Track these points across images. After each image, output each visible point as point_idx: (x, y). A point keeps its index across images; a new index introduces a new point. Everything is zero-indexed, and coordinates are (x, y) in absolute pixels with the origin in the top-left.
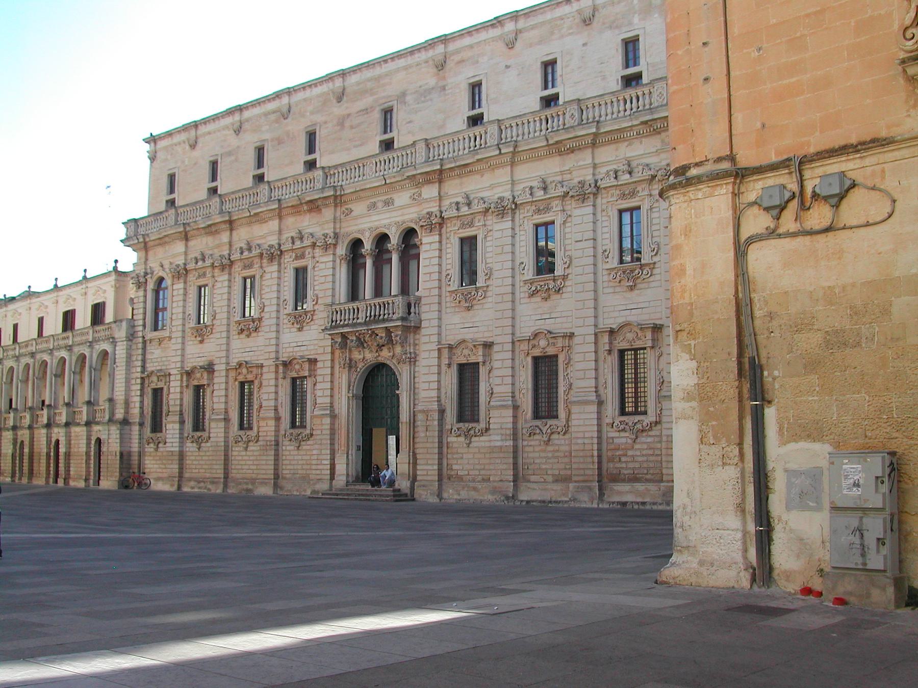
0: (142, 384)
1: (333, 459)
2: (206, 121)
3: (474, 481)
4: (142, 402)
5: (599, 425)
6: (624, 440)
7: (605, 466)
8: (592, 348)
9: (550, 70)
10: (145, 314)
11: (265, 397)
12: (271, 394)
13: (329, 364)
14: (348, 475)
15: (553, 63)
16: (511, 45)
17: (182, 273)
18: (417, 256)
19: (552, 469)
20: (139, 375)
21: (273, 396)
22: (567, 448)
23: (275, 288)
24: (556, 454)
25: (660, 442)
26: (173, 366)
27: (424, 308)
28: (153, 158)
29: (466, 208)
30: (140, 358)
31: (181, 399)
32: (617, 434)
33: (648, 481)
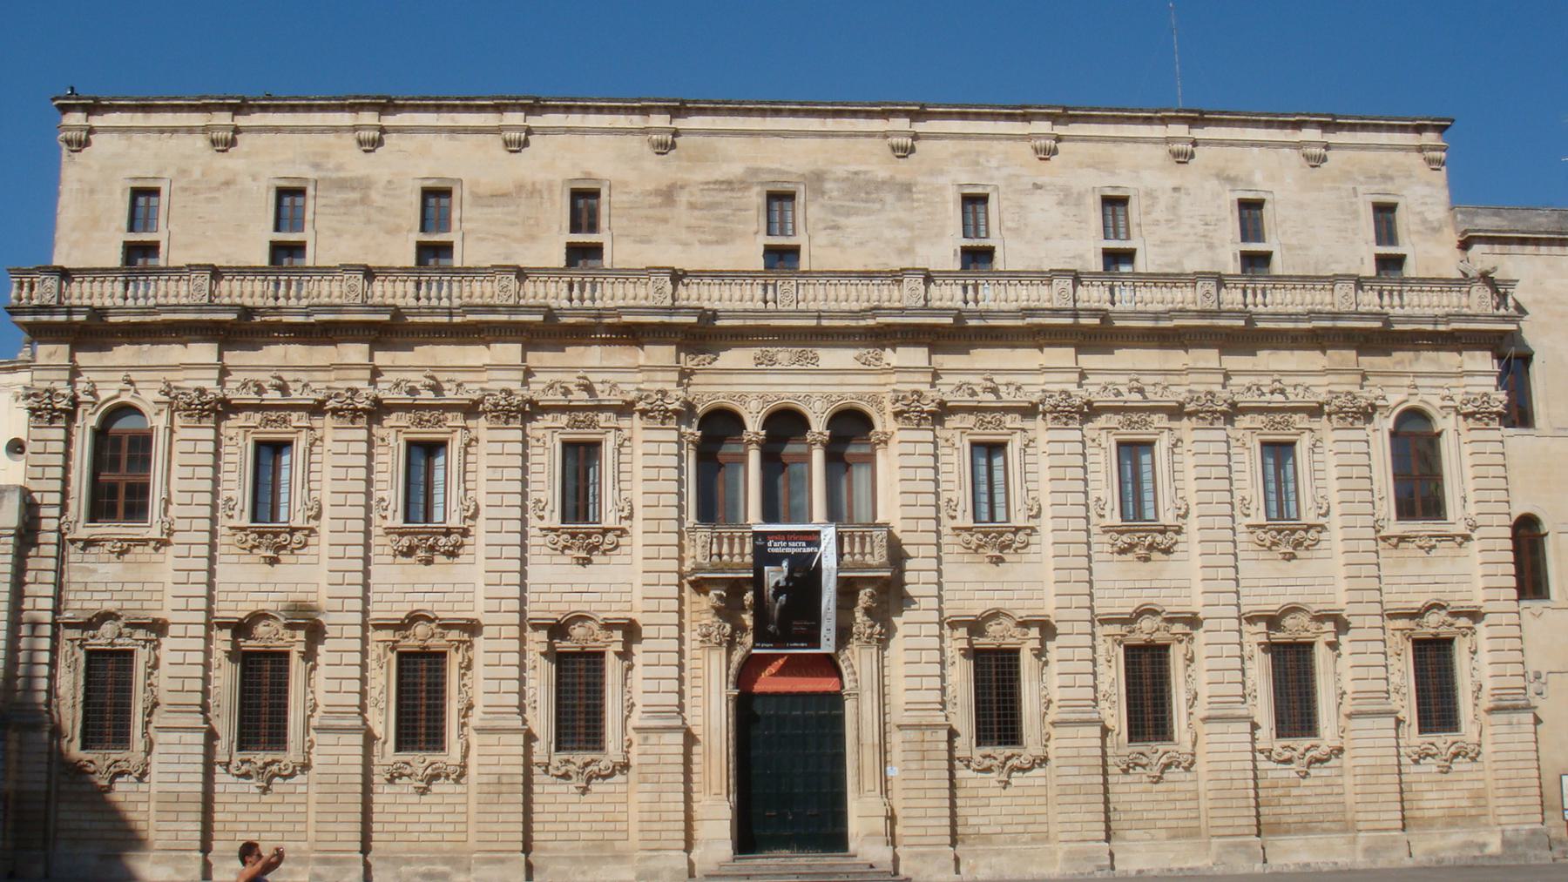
32: (1273, 765)
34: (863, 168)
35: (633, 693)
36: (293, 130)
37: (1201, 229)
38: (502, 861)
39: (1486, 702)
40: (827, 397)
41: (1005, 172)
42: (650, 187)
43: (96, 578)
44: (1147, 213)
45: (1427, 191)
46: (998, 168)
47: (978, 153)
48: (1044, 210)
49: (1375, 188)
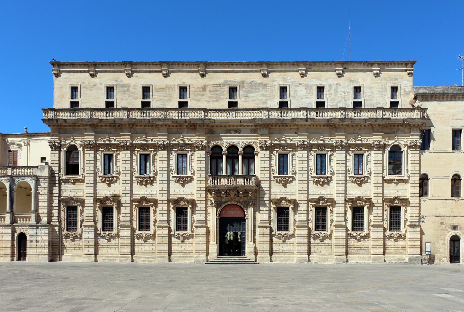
10: (59, 164)
34: (254, 80)
36: (110, 71)
37: (343, 95)
38: (163, 257)
39: (408, 223)
40: (243, 142)
41: (291, 80)
43: (68, 189)
44: (329, 91)
45: (407, 82)
46: (290, 79)
47: (285, 75)
48: (301, 91)
49: (392, 82)
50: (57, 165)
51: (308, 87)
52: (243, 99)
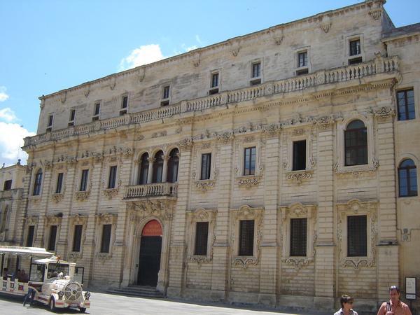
0: (24, 223)
1: (122, 271)
2: (71, 90)
3: (201, 288)
4: (23, 233)
5: (277, 261)
6: (291, 271)
7: (280, 285)
8: (275, 217)
9: (256, 68)
11: (87, 234)
12: (92, 233)
13: (124, 218)
14: (130, 280)
15: (258, 64)
16: (235, 55)
17: (50, 166)
18: (177, 163)
19: (248, 285)
20: (23, 218)
21: (92, 234)
22: (257, 273)
23: (98, 176)
24: (251, 276)
25: (314, 273)
26: (41, 214)
27: (179, 191)
28: (42, 108)
29: (206, 138)
30: (24, 209)
31: (43, 233)
32: (288, 267)
33: (306, 295)
35: (117, 234)
41: (225, 63)
42: (138, 92)
45: (373, 29)
48: (234, 73)
49: (350, 34)
50: (27, 188)
51: (242, 66)
52: (175, 97)
